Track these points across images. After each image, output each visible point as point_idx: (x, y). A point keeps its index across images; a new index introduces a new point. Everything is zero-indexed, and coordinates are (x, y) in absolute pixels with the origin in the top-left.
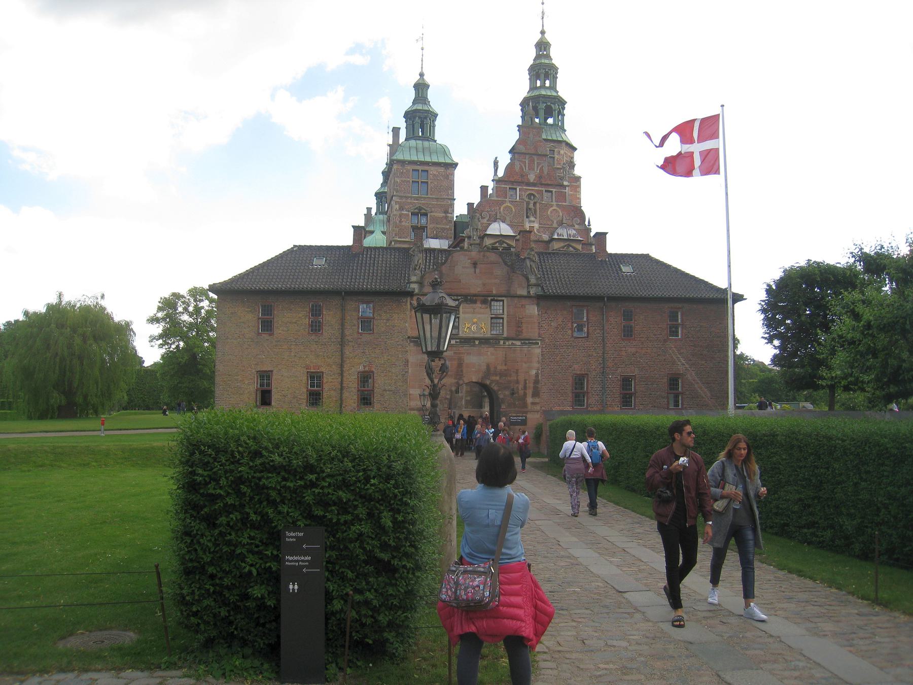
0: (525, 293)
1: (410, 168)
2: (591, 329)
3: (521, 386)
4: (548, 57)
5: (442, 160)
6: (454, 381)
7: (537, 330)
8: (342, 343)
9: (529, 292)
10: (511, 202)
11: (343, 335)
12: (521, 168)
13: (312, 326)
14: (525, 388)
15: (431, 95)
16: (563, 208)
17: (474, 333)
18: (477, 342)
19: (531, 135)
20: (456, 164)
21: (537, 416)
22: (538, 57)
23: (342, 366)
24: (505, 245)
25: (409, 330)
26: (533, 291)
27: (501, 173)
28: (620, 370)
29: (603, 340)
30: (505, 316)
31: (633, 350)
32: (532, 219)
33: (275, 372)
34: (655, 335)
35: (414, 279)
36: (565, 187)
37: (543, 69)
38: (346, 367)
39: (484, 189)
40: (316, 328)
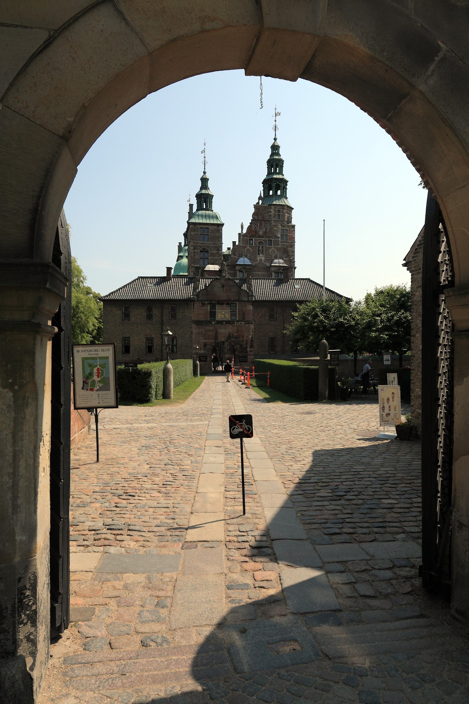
0: (246, 299)
1: (199, 226)
3: (245, 343)
5: (215, 222)
6: (214, 341)
8: (162, 324)
10: (250, 247)
11: (162, 320)
12: (255, 228)
14: (247, 344)
15: (210, 184)
16: (278, 249)
18: (224, 323)
20: (223, 224)
21: (252, 357)
22: (272, 155)
27: (245, 231)
30: (237, 311)
33: (131, 337)
36: (278, 238)
37: (275, 163)
39: (234, 243)
40: (150, 317)
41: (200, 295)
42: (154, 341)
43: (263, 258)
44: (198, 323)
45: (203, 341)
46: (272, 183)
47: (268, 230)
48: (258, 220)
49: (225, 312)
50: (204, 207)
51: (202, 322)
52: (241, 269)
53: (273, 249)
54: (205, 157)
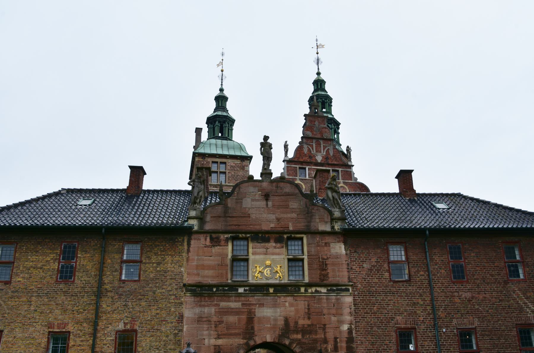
0: (328, 228)
2: (413, 270)
5: (238, 153)
7: (346, 274)
8: (99, 294)
9: (333, 228)
10: (301, 180)
11: (101, 283)
12: (309, 150)
13: (62, 272)
15: (229, 105)
17: (267, 278)
18: (271, 290)
19: (316, 123)
20: (251, 157)
22: (315, 91)
23: (95, 324)
25: (185, 276)
26: (337, 227)
27: (291, 155)
28: (455, 321)
29: (430, 283)
30: (305, 257)
31: (468, 295)
33: (6, 332)
34: (492, 275)
35: (193, 213)
38: (101, 325)
40: (66, 274)
41: (208, 218)
42: (71, 343)
44: (200, 291)
45: (213, 341)
47: (331, 153)
49: (273, 260)
51: (211, 286)
54: (222, 71)
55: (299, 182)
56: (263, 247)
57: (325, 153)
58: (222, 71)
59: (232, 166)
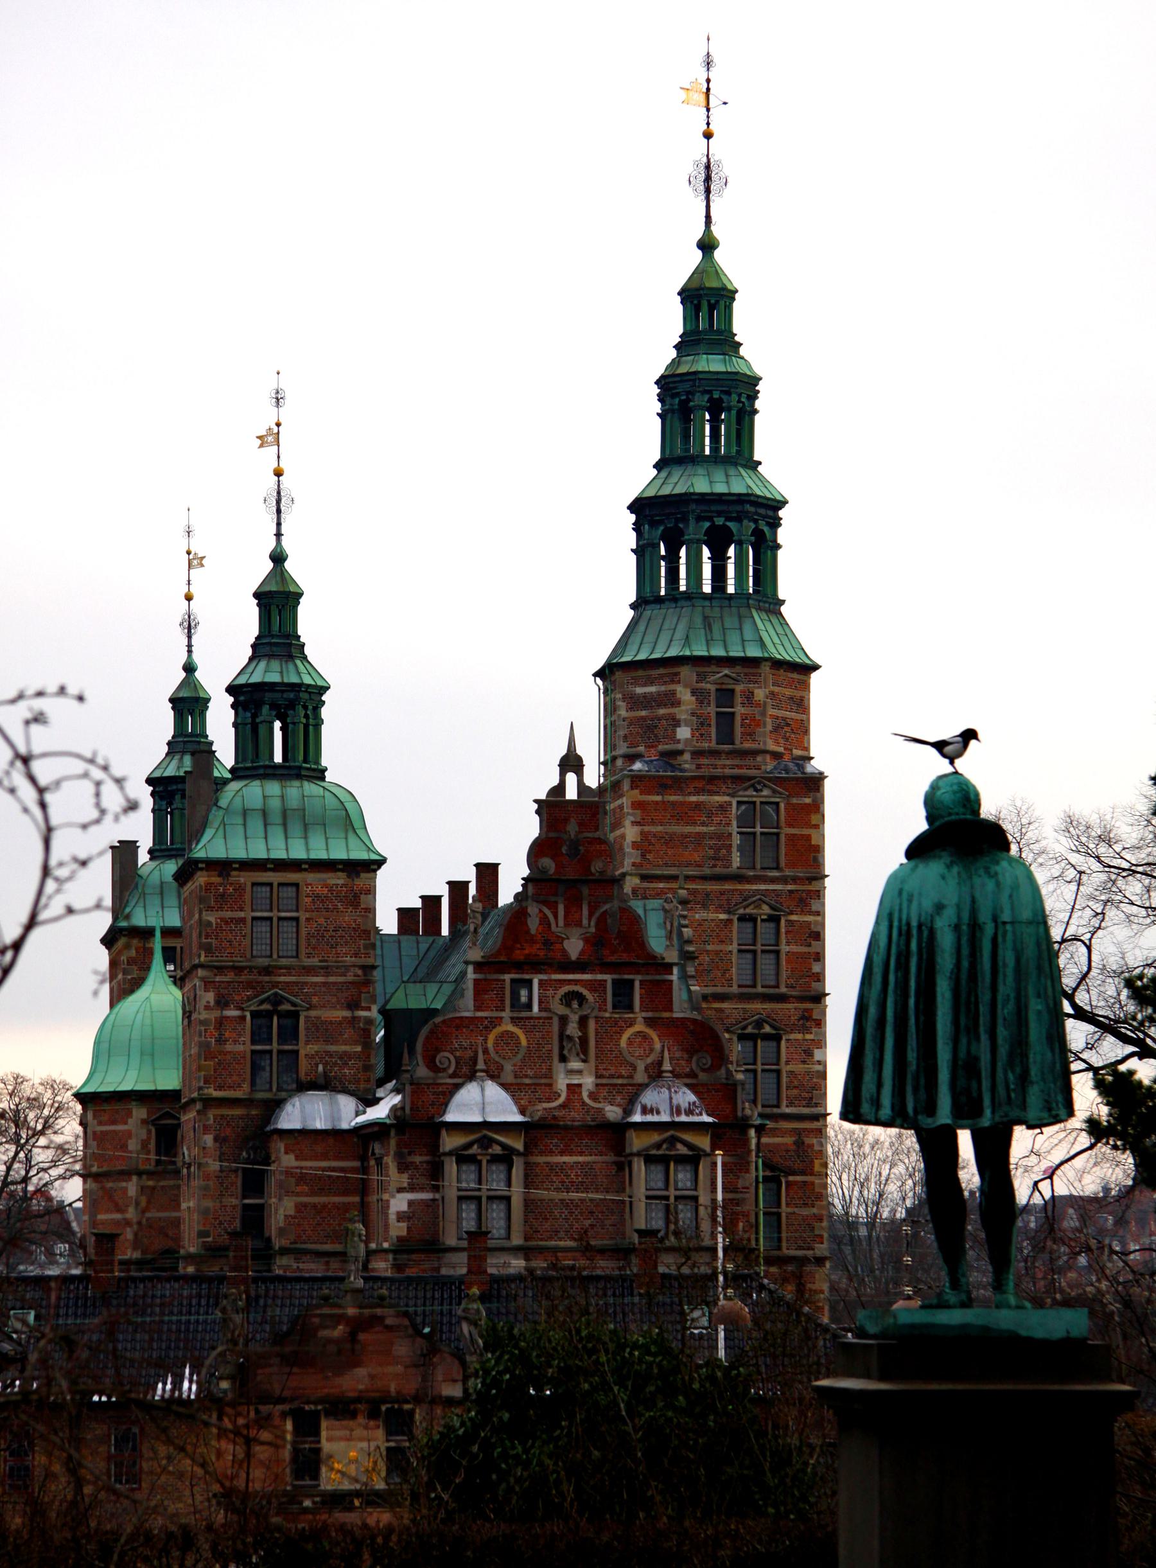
4: (728, 344)
5: (339, 853)
10: (514, 1020)
12: (544, 921)
15: (309, 623)
24: (497, 1149)
32: (575, 1065)
43: (588, 1081)
46: (685, 520)
48: (559, 881)
50: (278, 758)
52: (469, 1145)
53: (639, 1027)
54: (278, 473)
55: (511, 1028)
56: (346, 1428)
57: (593, 930)
58: (278, 473)
59: (318, 896)
